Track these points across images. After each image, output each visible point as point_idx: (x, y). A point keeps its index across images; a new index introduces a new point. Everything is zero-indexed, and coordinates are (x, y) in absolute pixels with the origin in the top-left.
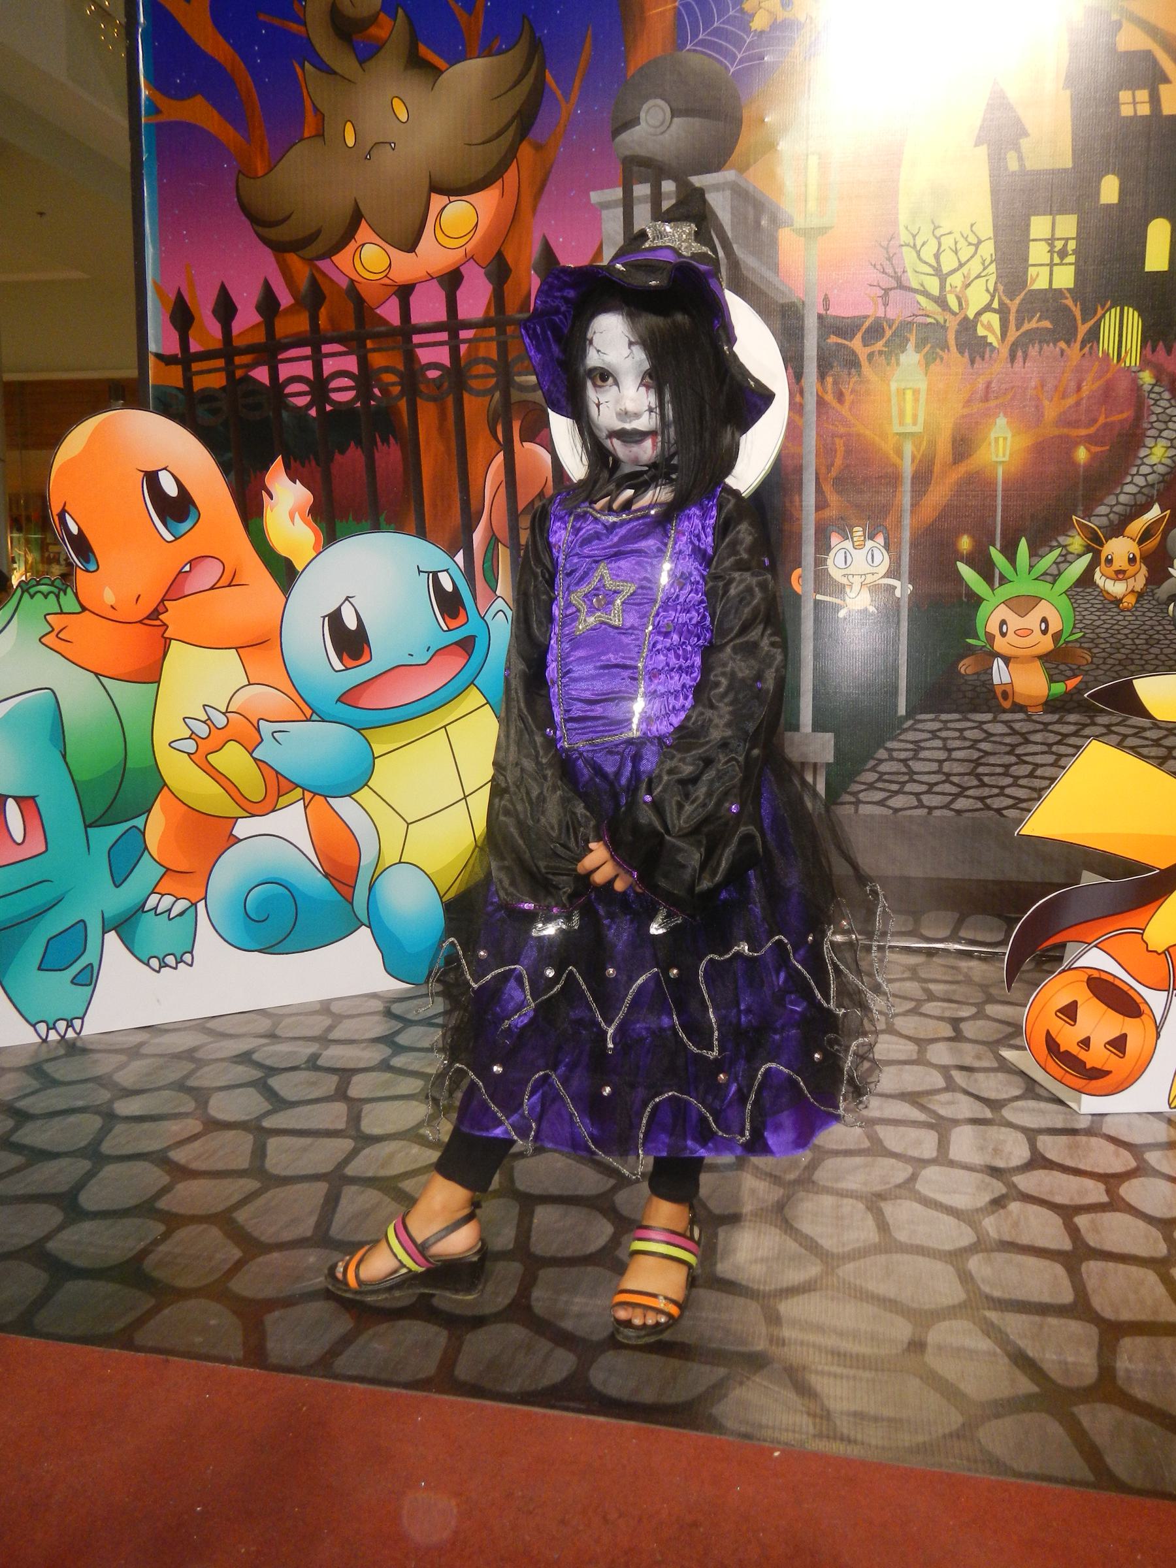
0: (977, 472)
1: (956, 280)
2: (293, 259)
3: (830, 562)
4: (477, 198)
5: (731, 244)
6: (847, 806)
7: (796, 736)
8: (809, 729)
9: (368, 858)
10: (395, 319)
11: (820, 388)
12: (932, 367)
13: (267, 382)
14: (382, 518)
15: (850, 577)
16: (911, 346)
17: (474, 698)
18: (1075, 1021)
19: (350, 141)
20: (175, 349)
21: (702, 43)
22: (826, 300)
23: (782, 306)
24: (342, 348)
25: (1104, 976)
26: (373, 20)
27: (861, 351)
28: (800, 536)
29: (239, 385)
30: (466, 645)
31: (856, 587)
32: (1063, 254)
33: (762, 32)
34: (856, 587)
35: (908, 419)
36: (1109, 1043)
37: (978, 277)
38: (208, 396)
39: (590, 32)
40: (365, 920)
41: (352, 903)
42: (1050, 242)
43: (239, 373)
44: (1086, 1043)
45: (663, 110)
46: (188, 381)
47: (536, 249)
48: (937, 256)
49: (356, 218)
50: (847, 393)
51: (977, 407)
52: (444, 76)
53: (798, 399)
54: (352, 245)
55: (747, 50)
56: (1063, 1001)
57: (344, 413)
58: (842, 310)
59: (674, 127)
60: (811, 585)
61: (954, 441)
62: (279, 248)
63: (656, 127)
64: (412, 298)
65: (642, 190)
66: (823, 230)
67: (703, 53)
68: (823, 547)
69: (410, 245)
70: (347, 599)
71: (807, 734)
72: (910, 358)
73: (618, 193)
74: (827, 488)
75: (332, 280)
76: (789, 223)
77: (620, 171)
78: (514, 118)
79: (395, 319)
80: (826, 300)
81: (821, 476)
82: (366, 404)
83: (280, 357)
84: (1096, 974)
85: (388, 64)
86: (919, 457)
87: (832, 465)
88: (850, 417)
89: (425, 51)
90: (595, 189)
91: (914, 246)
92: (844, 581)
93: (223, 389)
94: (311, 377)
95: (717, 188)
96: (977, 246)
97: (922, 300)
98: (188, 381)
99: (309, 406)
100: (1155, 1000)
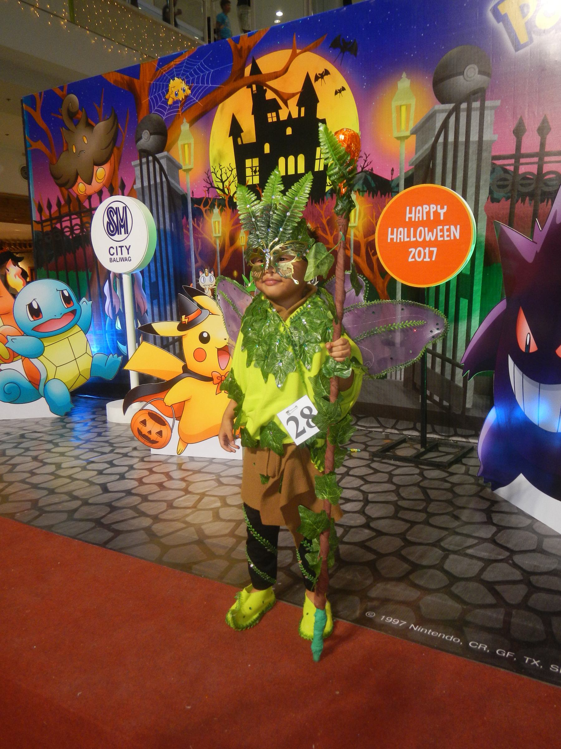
0: (237, 249)
1: (226, 183)
2: (63, 189)
3: (200, 281)
4: (104, 166)
9: (43, 377)
10: (88, 207)
12: (222, 213)
13: (60, 228)
14: (89, 270)
16: (216, 207)
17: (77, 329)
18: (146, 425)
19: (74, 152)
20: (39, 219)
21: (157, 111)
22: (193, 192)
24: (76, 217)
25: (153, 412)
26: (77, 113)
27: (203, 209)
28: (191, 272)
29: (54, 229)
30: (74, 312)
31: (207, 289)
32: (255, 172)
33: (170, 105)
34: (207, 289)
35: (217, 231)
36: (157, 433)
37: (233, 182)
38: (47, 233)
40: (43, 395)
41: (38, 390)
42: (252, 168)
43: (54, 226)
44: (150, 432)
46: (42, 229)
47: (119, 183)
48: (221, 175)
49: (77, 174)
51: (235, 227)
52: (95, 128)
54: (77, 184)
56: (142, 419)
57: (78, 236)
58: (196, 196)
59: (151, 138)
61: (230, 239)
62: (61, 186)
64: (92, 200)
65: (144, 160)
66: (190, 170)
68: (198, 276)
69: (90, 183)
70: (34, 299)
72: (216, 211)
73: (138, 162)
75: (73, 196)
76: (181, 168)
77: (138, 154)
79: (88, 207)
80: (193, 192)
82: (83, 234)
83: (63, 220)
84: (151, 412)
85: (81, 126)
86: (221, 244)
88: (202, 232)
89: (90, 121)
91: (215, 173)
92: (204, 287)
93: (50, 231)
94: (69, 225)
95: (162, 158)
96: (232, 171)
97: (218, 190)
98: (42, 229)
99: (69, 236)
100: (170, 421)
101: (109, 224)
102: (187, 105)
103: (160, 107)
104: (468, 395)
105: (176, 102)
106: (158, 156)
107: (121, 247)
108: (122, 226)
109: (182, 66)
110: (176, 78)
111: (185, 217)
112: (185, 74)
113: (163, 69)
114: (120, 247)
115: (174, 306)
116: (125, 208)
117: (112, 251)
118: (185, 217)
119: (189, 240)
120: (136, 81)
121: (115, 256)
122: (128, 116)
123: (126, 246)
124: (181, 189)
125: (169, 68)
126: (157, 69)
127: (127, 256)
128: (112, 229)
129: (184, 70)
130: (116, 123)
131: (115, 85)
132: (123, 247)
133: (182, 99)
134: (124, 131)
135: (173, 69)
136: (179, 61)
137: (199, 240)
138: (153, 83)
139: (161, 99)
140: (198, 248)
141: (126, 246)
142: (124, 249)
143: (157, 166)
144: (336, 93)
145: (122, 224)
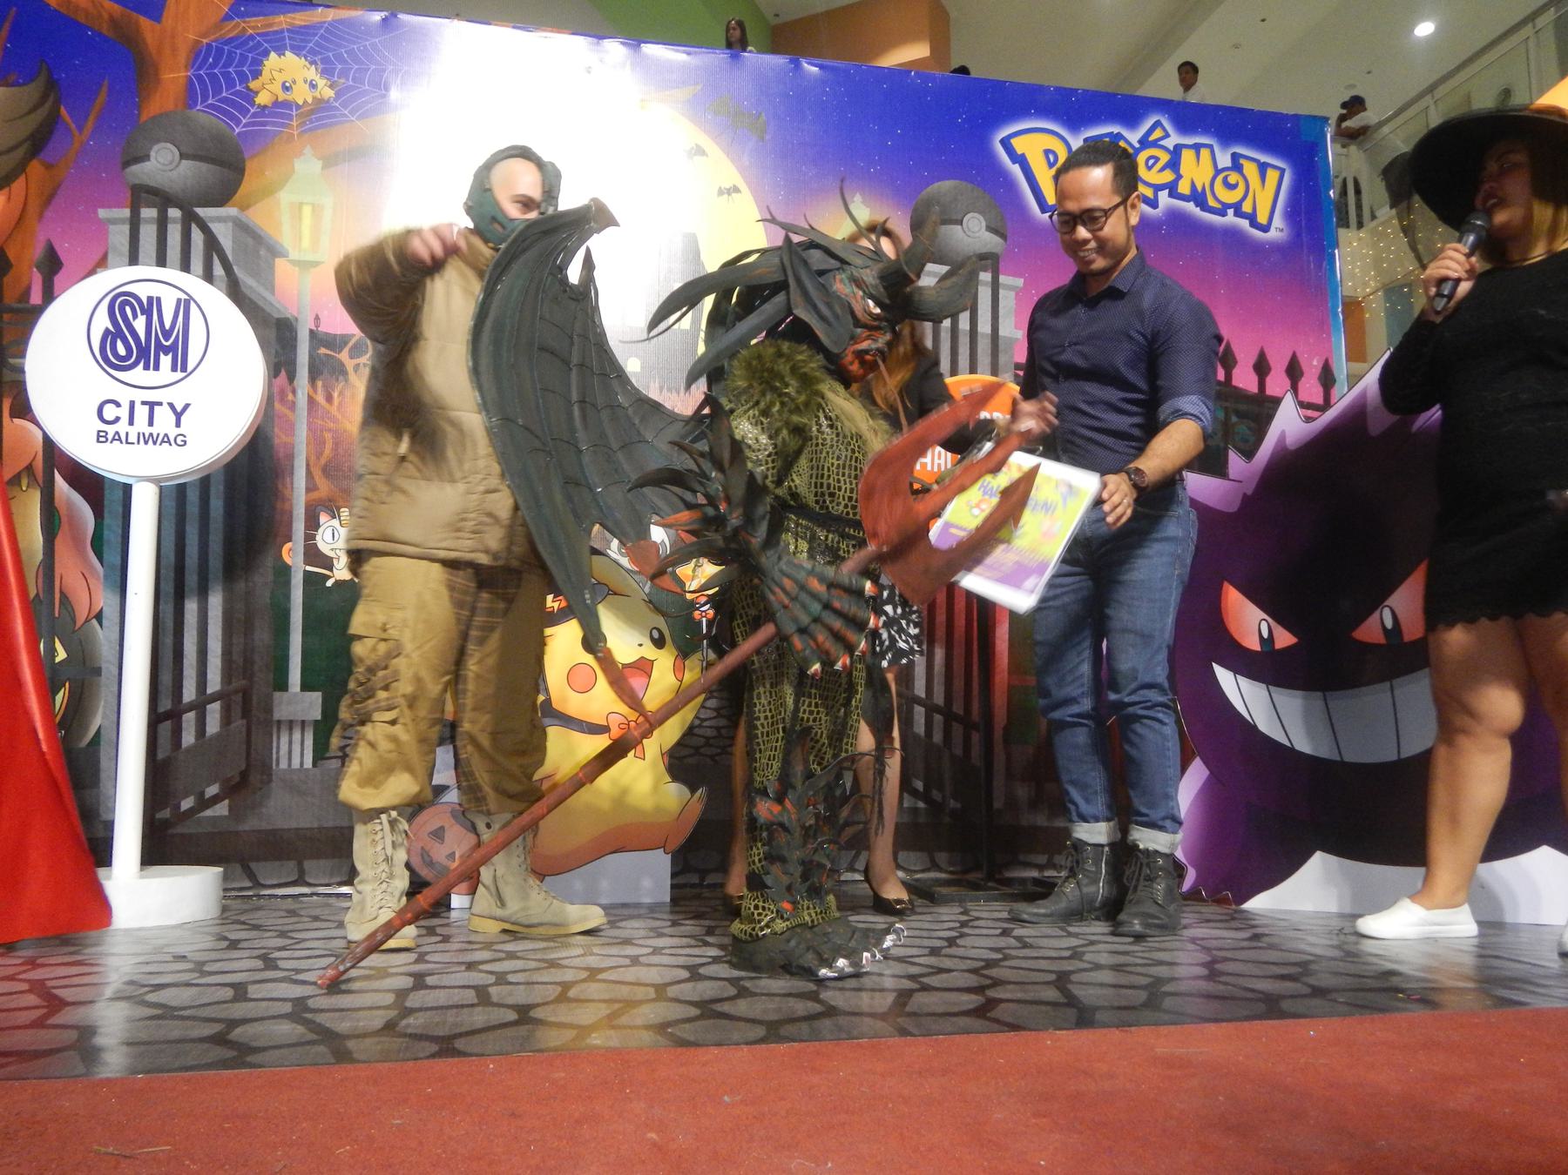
3: (318, 538)
5: (231, 266)
6: (334, 760)
7: (285, 695)
8: (298, 689)
11: (311, 390)
15: (338, 551)
21: (211, 106)
22: (317, 318)
23: (278, 320)
27: (349, 364)
33: (265, 107)
39: (106, 82)
45: (174, 156)
47: (38, 252)
50: (336, 395)
53: (290, 397)
55: (251, 117)
60: (301, 557)
63: (164, 165)
66: (316, 264)
67: (213, 115)
68: (313, 524)
71: (296, 694)
73: (126, 212)
74: (317, 473)
77: (129, 195)
78: (25, 141)
80: (317, 318)
81: (311, 463)
87: (321, 454)
90: (103, 207)
92: (331, 554)
95: (219, 219)
101: (110, 337)
102: (318, 120)
103: (222, 100)
104: (995, 783)
105: (281, 108)
106: (201, 211)
107: (152, 405)
108: (166, 350)
109: (316, 35)
110: (288, 53)
111: (283, 373)
112: (320, 53)
113: (249, 22)
114: (144, 403)
115: (216, 601)
116: (184, 306)
117: (110, 411)
118: (283, 373)
119: (290, 428)
120: (145, 23)
121: (122, 427)
122: (102, 97)
123: (171, 406)
124: (277, 305)
125: (271, 25)
126: (227, 18)
127: (173, 432)
128: (122, 350)
129: (318, 44)
130: (48, 105)
131: (61, 10)
132: (160, 404)
133: (305, 102)
134: (80, 129)
135: (282, 31)
136: (305, 21)
137: (328, 436)
138: (209, 45)
139: (231, 84)
140: (319, 455)
141: (171, 406)
142: (163, 414)
143: (197, 236)
144: (721, 192)
145: (167, 344)
